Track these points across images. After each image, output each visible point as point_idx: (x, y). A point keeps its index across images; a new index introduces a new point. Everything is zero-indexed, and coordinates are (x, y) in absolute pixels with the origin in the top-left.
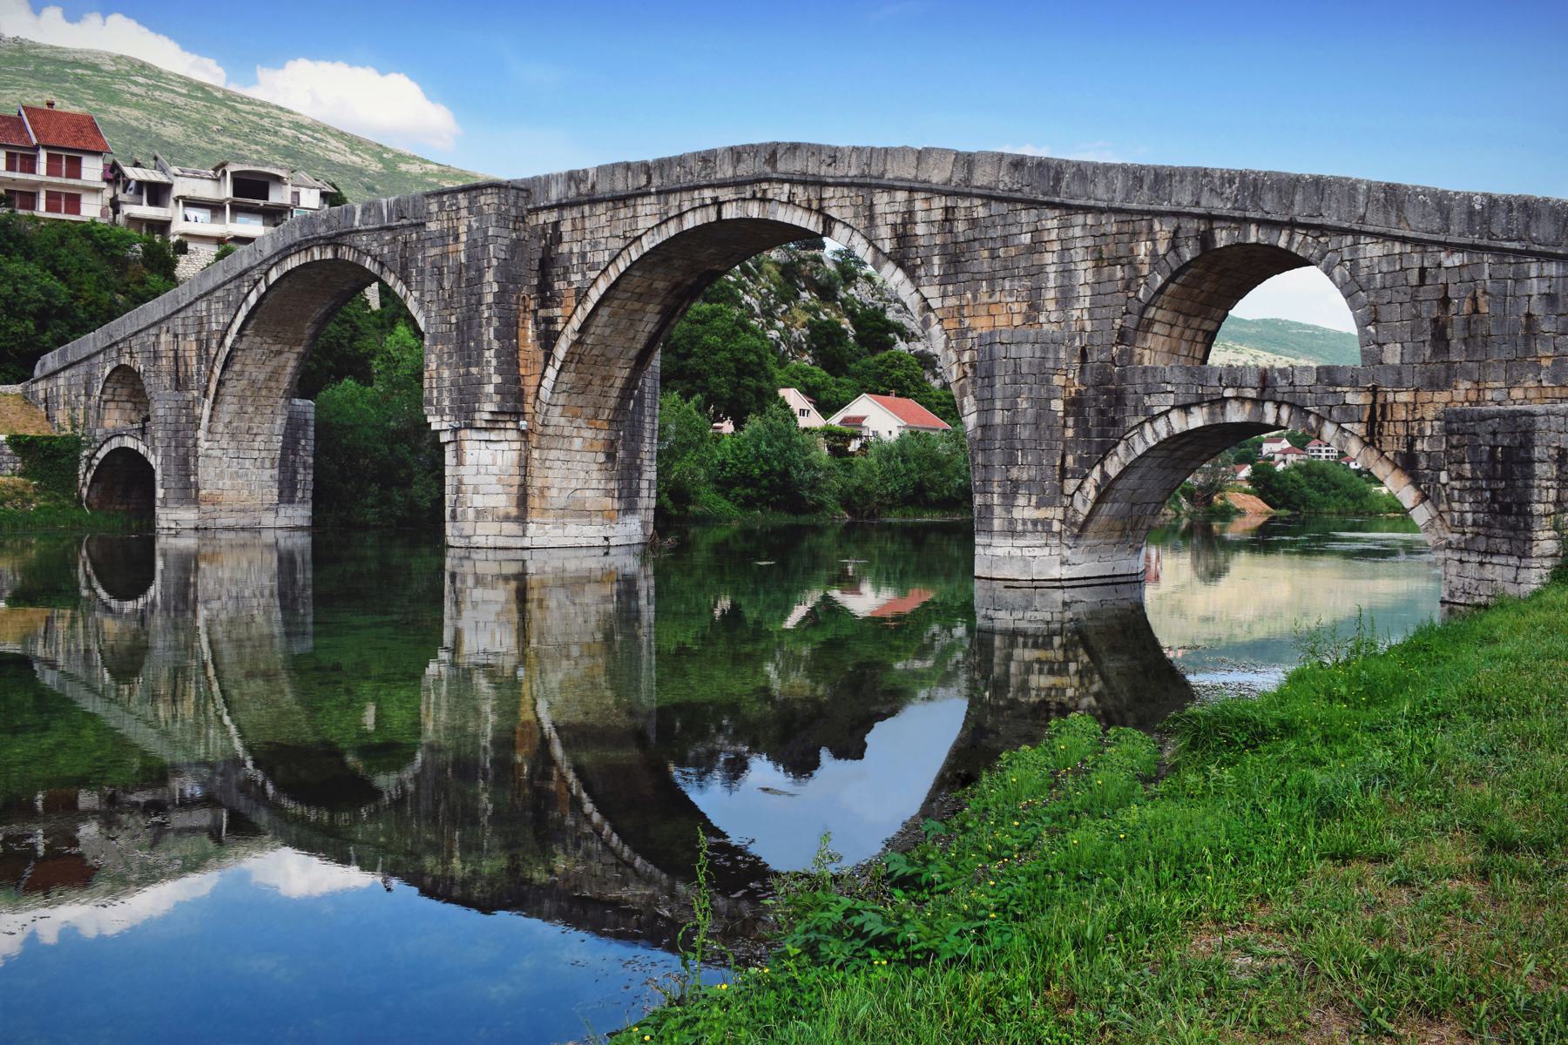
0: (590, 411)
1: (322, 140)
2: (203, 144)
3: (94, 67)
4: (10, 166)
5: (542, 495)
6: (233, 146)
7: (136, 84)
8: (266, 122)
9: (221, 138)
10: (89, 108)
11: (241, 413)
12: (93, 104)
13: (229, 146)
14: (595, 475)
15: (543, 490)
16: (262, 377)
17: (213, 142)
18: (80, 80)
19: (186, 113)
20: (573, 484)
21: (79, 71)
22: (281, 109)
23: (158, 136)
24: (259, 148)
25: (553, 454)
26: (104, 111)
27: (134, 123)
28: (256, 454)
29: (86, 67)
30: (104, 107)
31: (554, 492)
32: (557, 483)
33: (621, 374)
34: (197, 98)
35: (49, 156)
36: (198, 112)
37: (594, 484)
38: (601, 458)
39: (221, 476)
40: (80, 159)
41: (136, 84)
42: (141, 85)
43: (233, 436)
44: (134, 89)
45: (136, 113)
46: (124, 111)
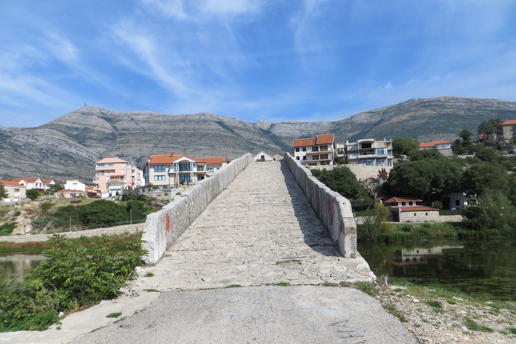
1: (507, 105)
2: (471, 114)
3: (439, 101)
4: (313, 151)
6: (479, 113)
7: (450, 102)
8: (489, 104)
9: (476, 112)
10: (438, 111)
12: (439, 110)
13: (478, 113)
17: (473, 113)
18: (436, 105)
19: (465, 107)
21: (435, 103)
22: (493, 100)
23: (458, 115)
24: (487, 112)
26: (441, 111)
27: (450, 113)
29: (437, 101)
30: (442, 110)
34: (468, 102)
35: (320, 147)
36: (468, 106)
40: (327, 146)
41: (450, 102)
42: (452, 102)
44: (450, 104)
45: (451, 110)
46: (448, 110)
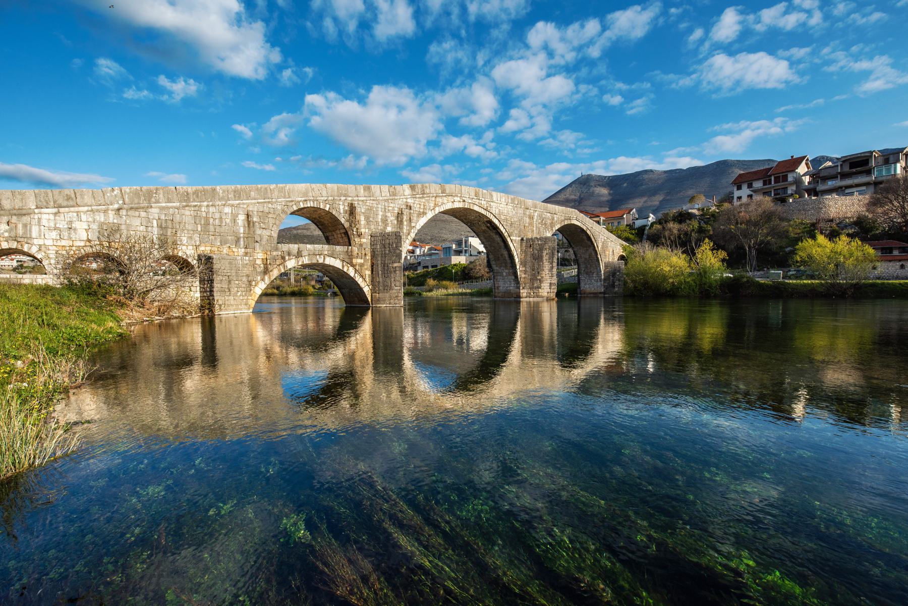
0: (503, 265)
5: (498, 289)
11: (586, 267)
14: (513, 283)
15: (498, 287)
16: (587, 257)
20: (506, 285)
25: (499, 277)
28: (595, 278)
31: (501, 288)
32: (502, 285)
33: (505, 253)
37: (513, 285)
38: (513, 278)
39: (585, 284)
43: (587, 274)
